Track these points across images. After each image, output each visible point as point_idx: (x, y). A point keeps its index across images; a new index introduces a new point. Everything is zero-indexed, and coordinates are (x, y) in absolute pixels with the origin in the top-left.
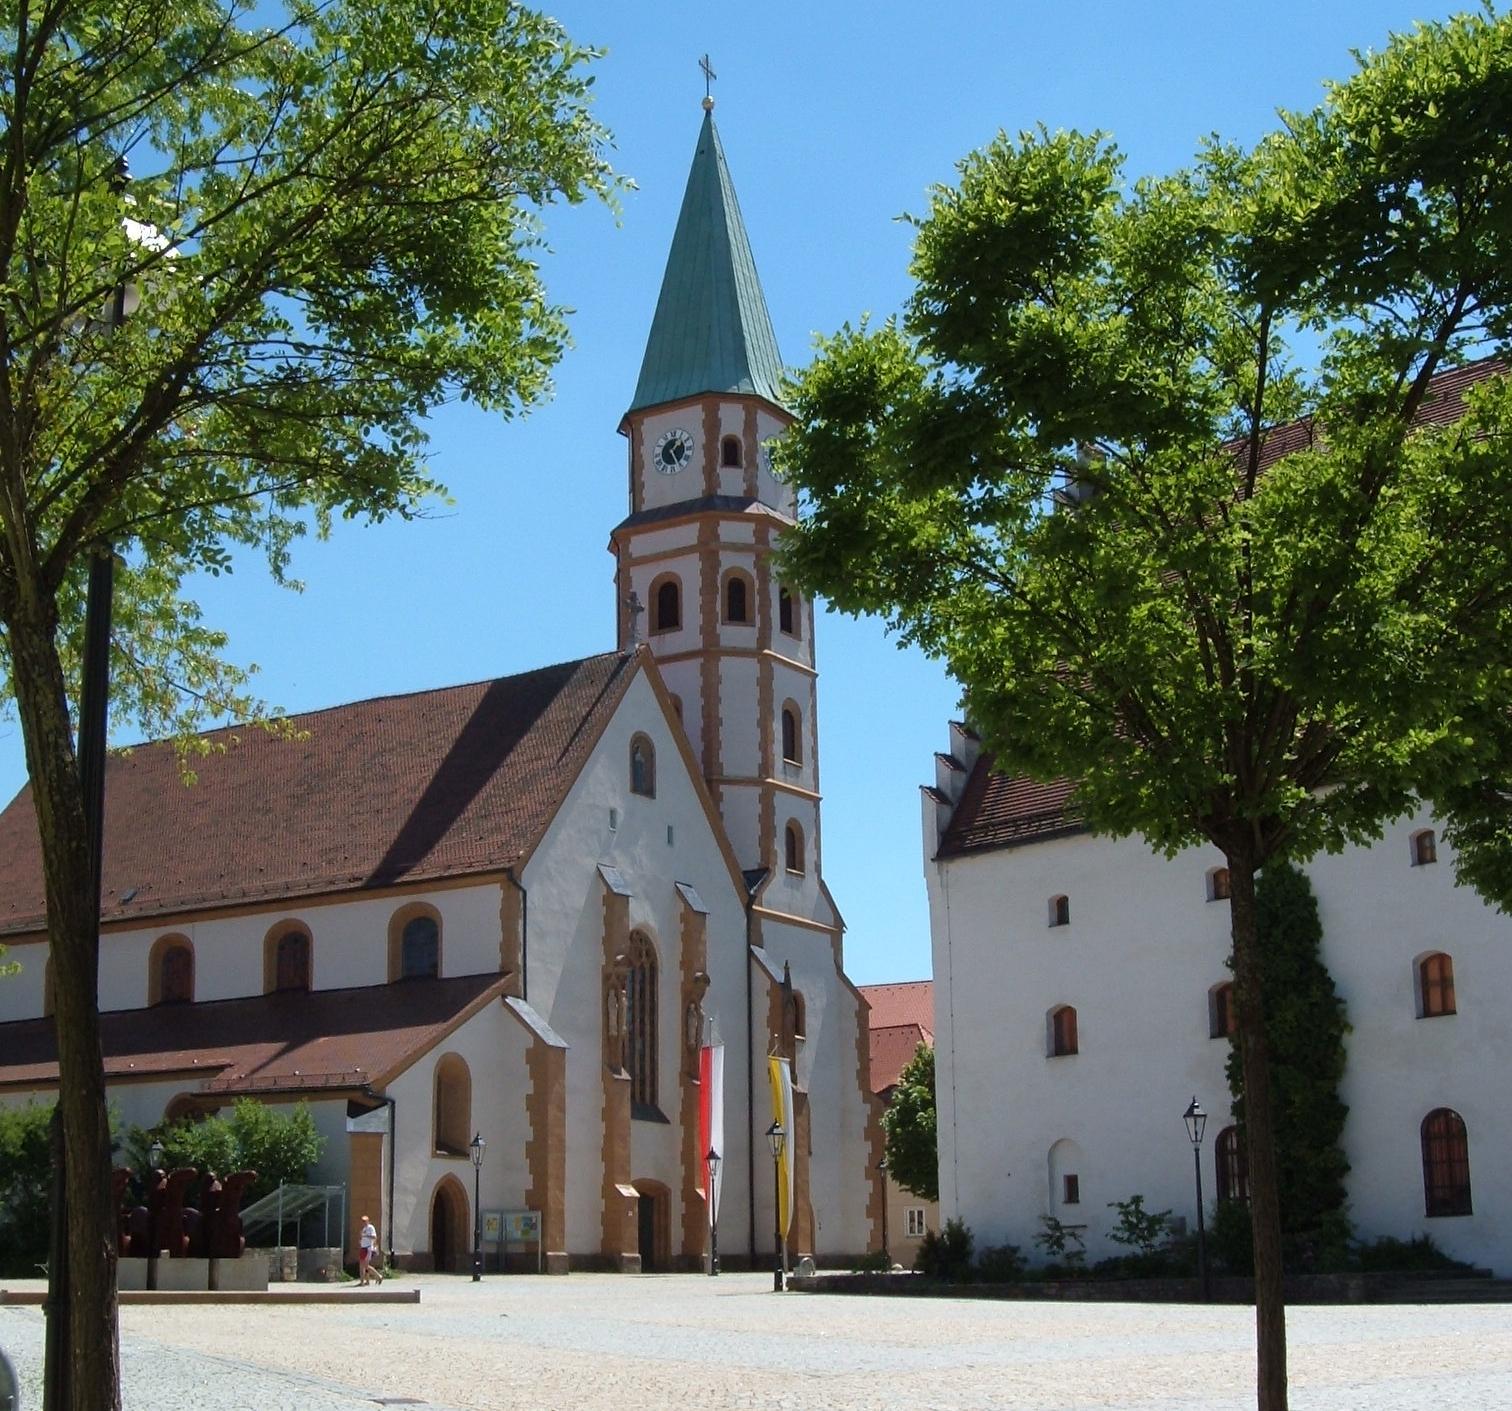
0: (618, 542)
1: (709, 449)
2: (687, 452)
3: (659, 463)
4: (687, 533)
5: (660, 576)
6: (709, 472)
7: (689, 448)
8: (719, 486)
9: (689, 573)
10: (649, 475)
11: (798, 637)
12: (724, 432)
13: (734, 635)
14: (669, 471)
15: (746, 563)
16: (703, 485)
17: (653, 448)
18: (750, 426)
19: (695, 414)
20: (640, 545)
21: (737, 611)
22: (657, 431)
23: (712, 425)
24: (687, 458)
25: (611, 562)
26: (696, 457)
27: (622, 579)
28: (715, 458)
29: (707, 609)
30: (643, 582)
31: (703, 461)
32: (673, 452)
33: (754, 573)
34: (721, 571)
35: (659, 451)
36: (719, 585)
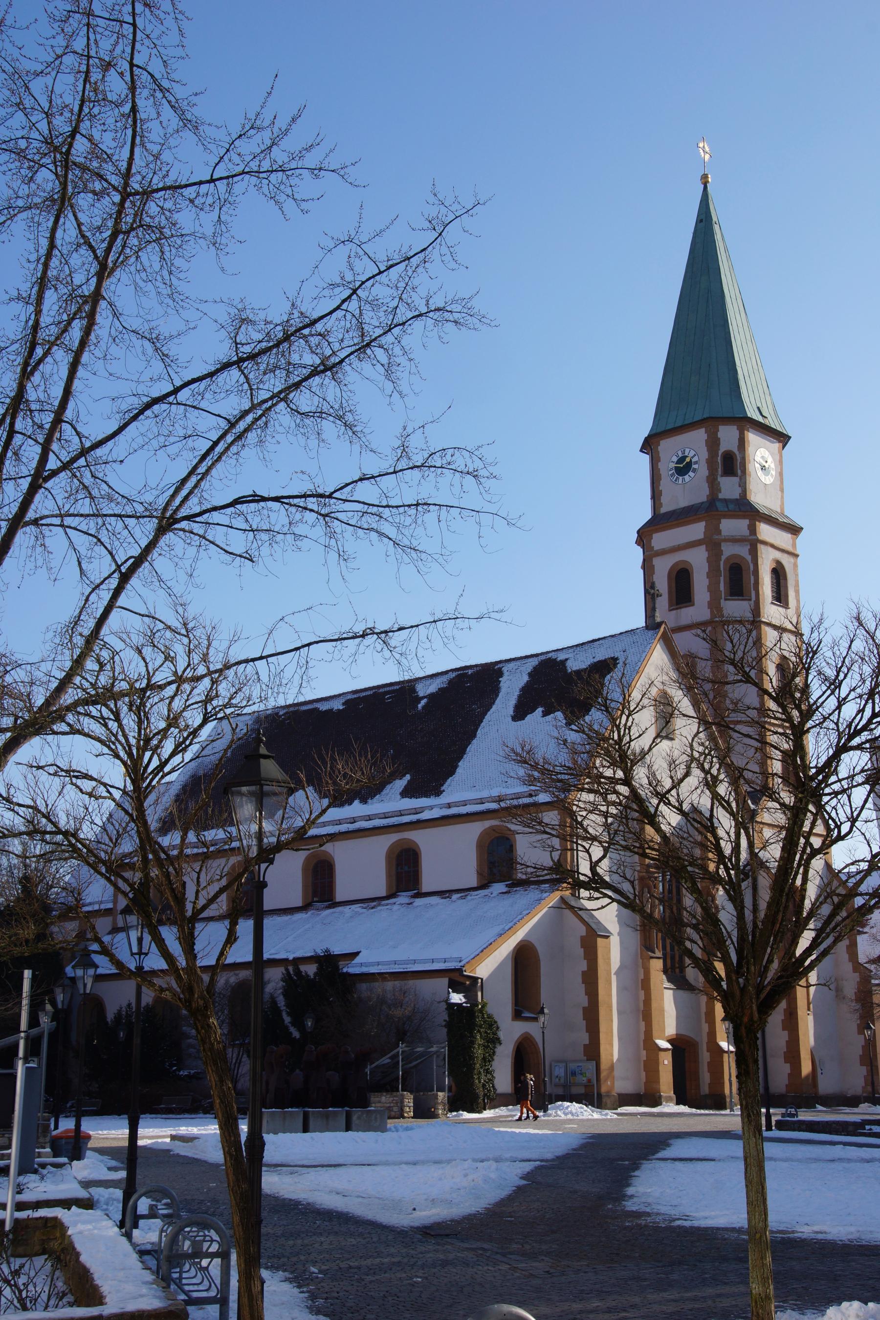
0: (644, 536)
2: (694, 466)
3: (672, 475)
4: (696, 530)
5: (676, 564)
6: (712, 481)
7: (696, 463)
9: (698, 559)
10: (665, 484)
11: (786, 606)
12: (723, 448)
13: (735, 608)
14: (680, 482)
15: (743, 551)
17: (668, 463)
18: (742, 443)
19: (699, 436)
20: (660, 540)
22: (671, 450)
23: (713, 443)
24: (694, 471)
25: (638, 553)
26: (702, 469)
27: (647, 567)
28: (717, 470)
29: (713, 589)
30: (663, 566)
31: (706, 473)
33: (749, 558)
34: (723, 558)
36: (722, 569)
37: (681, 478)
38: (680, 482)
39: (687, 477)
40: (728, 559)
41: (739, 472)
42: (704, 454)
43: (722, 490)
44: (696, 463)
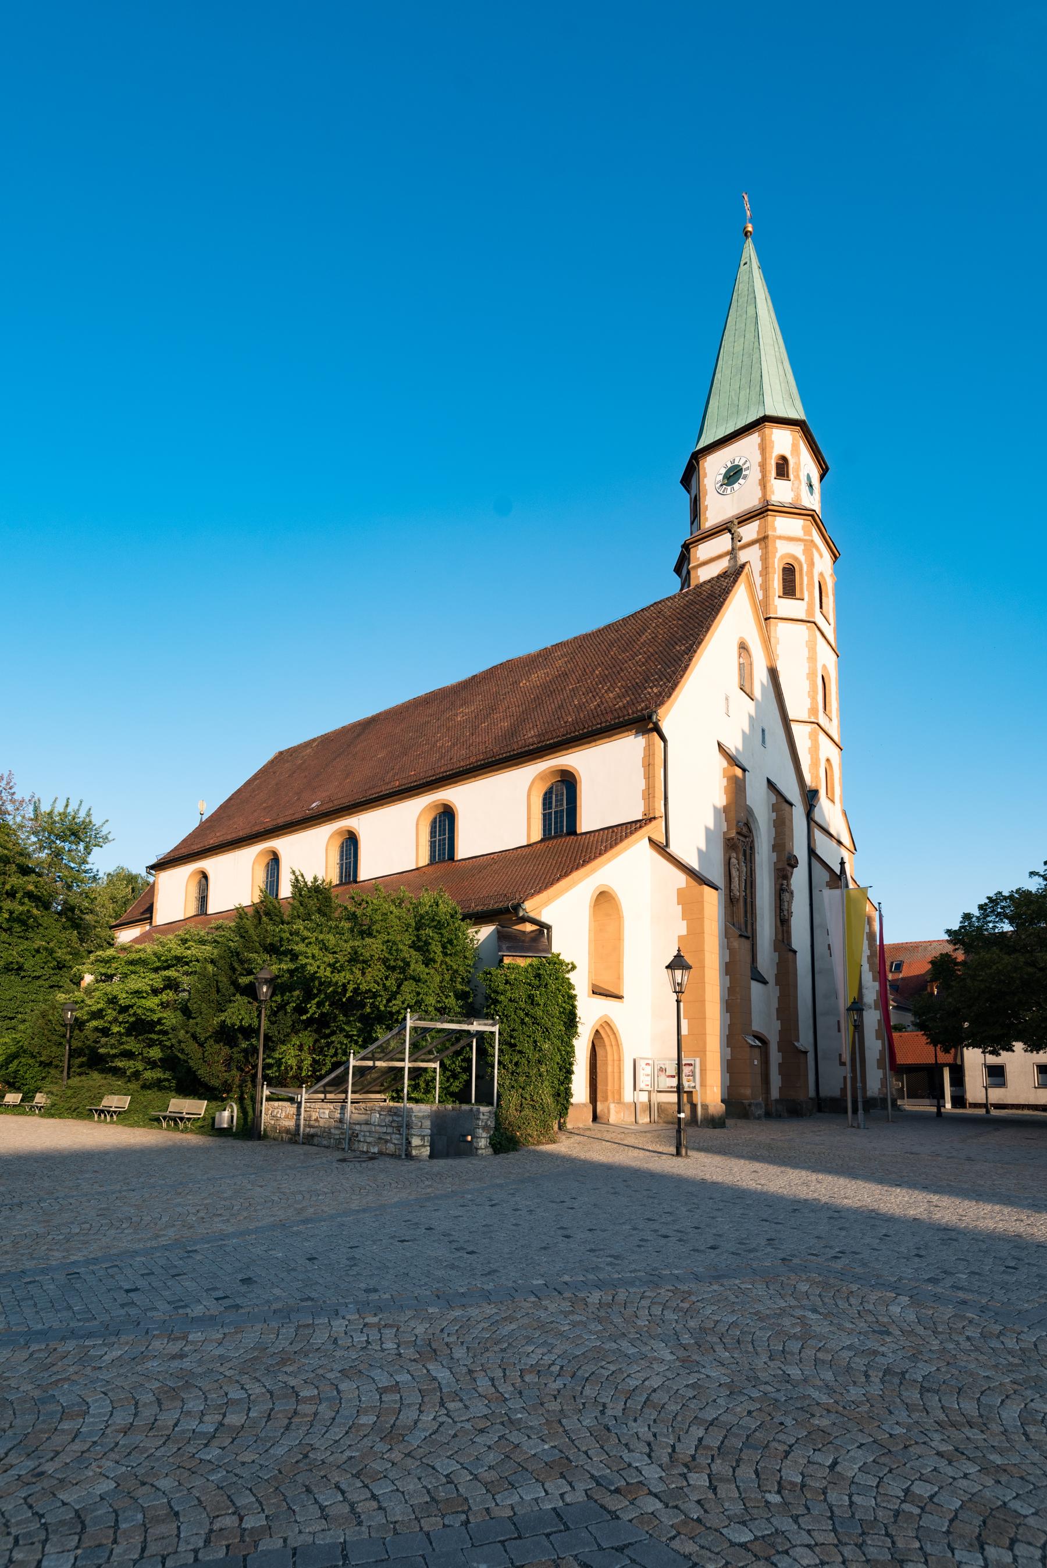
1: (763, 466)
2: (744, 473)
6: (763, 484)
7: (748, 468)
8: (773, 493)
13: (785, 607)
15: (797, 550)
16: (759, 494)
19: (752, 440)
21: (790, 589)
24: (745, 477)
26: (753, 475)
32: (733, 475)
34: (778, 555)
35: (721, 477)
36: (776, 566)
37: (729, 488)
38: (729, 492)
39: (736, 486)
40: (782, 558)
41: (791, 476)
42: (756, 457)
43: (776, 492)
44: (748, 468)
